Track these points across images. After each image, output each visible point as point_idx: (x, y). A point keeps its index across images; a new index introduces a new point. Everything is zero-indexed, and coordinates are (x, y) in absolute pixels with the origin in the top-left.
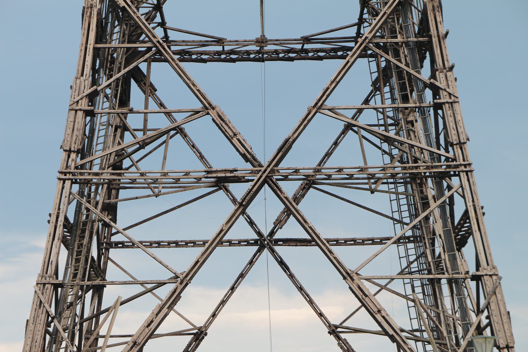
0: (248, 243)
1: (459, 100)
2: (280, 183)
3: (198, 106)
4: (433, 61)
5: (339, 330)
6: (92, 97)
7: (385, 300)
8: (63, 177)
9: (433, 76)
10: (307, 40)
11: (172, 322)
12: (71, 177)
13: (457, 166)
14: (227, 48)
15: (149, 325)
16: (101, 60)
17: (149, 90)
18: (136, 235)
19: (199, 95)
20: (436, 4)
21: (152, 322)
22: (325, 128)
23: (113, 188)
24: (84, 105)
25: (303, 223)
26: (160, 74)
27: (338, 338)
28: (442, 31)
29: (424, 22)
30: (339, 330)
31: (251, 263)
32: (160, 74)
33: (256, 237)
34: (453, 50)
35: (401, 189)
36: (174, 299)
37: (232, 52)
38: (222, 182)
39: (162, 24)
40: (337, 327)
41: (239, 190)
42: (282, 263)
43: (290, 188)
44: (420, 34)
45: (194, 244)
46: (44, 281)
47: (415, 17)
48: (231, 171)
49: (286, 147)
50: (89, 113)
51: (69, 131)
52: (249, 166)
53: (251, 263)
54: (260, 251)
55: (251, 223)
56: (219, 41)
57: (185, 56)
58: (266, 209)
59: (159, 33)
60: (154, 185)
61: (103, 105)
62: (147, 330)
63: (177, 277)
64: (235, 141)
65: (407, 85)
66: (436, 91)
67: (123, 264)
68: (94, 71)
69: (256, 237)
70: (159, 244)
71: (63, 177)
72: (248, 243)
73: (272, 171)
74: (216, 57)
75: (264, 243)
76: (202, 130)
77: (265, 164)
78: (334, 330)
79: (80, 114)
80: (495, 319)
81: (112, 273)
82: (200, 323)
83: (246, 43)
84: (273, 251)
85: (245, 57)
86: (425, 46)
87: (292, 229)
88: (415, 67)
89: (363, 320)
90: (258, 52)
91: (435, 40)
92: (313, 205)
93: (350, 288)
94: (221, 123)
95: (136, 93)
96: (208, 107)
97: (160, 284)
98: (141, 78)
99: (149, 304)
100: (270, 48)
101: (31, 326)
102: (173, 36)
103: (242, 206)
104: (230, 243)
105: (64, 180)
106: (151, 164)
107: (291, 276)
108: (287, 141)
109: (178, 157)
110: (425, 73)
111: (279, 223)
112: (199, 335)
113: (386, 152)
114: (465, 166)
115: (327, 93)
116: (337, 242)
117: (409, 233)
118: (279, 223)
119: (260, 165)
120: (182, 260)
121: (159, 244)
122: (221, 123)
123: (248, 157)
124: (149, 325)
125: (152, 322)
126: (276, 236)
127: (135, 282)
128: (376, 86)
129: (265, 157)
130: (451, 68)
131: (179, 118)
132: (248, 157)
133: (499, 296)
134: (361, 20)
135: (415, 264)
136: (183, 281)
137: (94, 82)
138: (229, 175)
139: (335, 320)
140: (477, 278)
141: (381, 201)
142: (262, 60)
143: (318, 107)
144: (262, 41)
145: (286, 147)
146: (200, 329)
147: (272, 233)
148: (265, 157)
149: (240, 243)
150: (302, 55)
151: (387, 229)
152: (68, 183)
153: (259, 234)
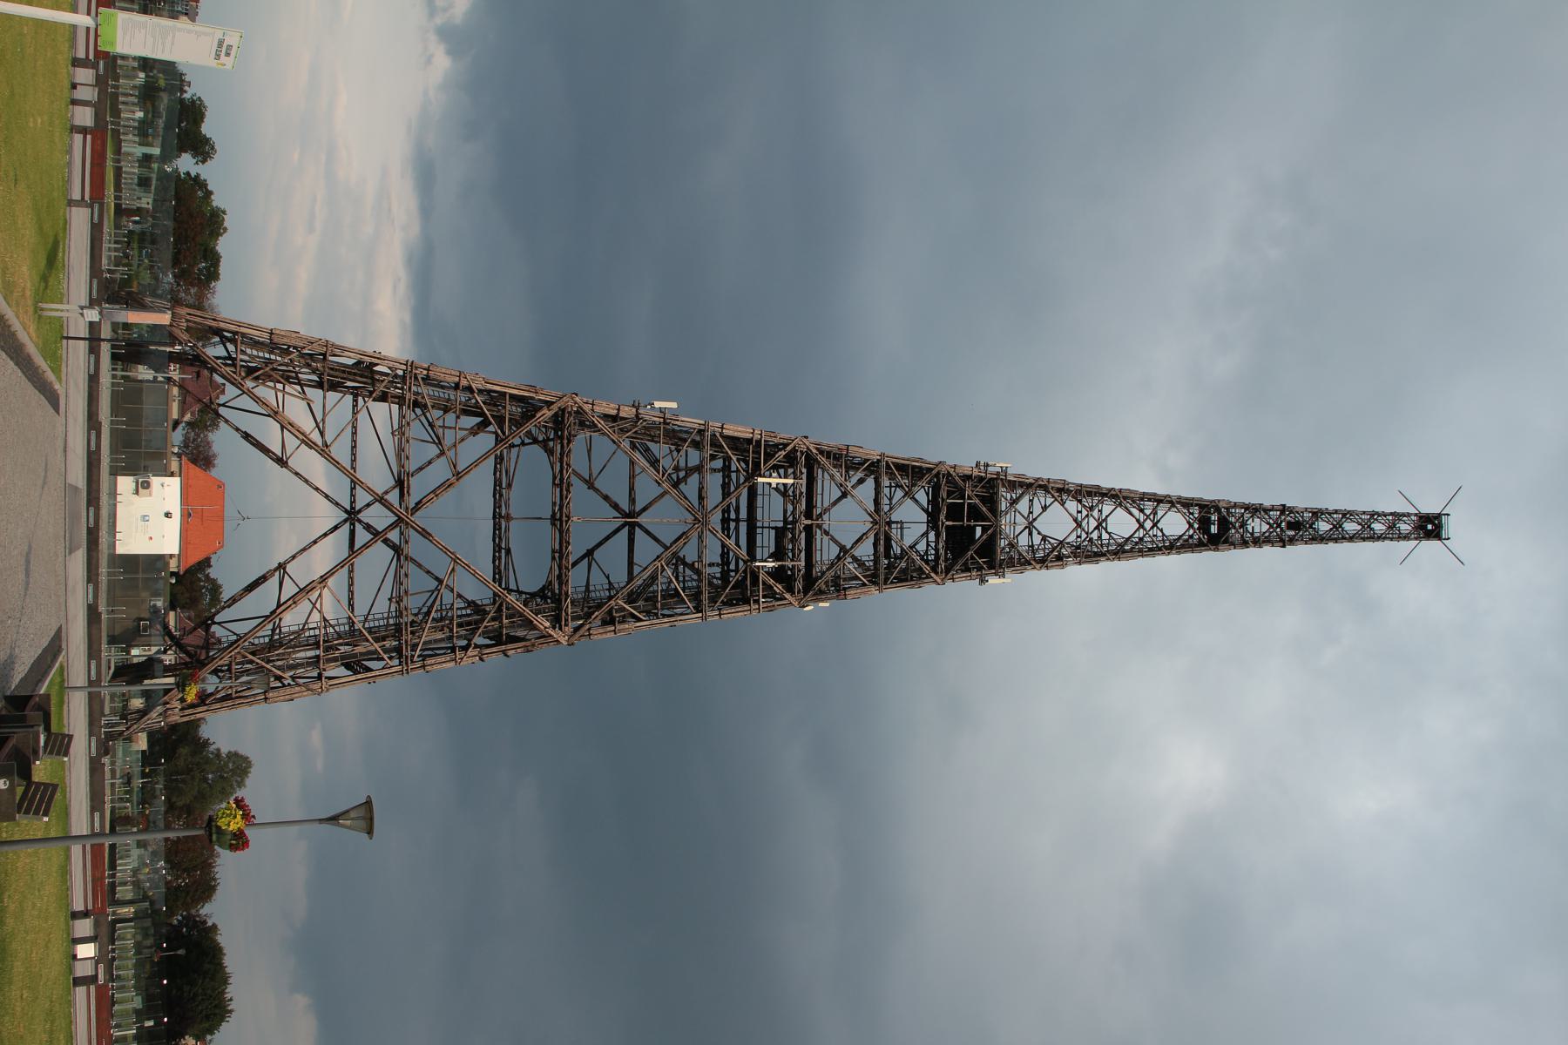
0: (353, 502)
3: (460, 468)
4: (488, 646)
6: (469, 389)
7: (305, 606)
9: (476, 646)
10: (508, 551)
11: (292, 443)
16: (495, 398)
17: (474, 431)
18: (363, 416)
19: (468, 470)
23: (401, 400)
24: (464, 383)
25: (366, 546)
26: (486, 441)
31: (337, 504)
32: (486, 441)
34: (494, 658)
35: (391, 621)
36: (311, 444)
38: (401, 484)
39: (523, 444)
41: (393, 498)
42: (336, 528)
43: (394, 536)
47: (520, 633)
49: (425, 534)
50: (457, 386)
52: (412, 505)
53: (337, 504)
54: (346, 511)
55: (368, 505)
56: (509, 486)
57: (499, 459)
58: (378, 517)
59: (517, 441)
60: (400, 431)
61: (463, 396)
65: (472, 627)
66: (465, 649)
67: (339, 405)
68: (489, 391)
70: (354, 433)
72: (353, 502)
74: (498, 482)
75: (352, 515)
76: (440, 472)
80: (288, 690)
81: (333, 396)
83: (507, 506)
84: (345, 521)
85: (497, 505)
86: (499, 639)
87: (362, 536)
89: (289, 590)
92: (380, 555)
94: (447, 485)
95: (470, 421)
96: (458, 475)
97: (322, 434)
98: (485, 424)
99: (307, 425)
102: (514, 451)
103: (381, 499)
104: (353, 489)
106: (417, 430)
109: (422, 451)
110: (478, 640)
111: (368, 527)
112: (282, 462)
115: (467, 567)
116: (351, 571)
118: (368, 527)
120: (341, 452)
121: (354, 433)
122: (447, 485)
123: (419, 505)
127: (324, 415)
128: (471, 604)
129: (419, 519)
131: (451, 454)
132: (419, 505)
134: (520, 593)
136: (324, 451)
137: (480, 391)
139: (289, 568)
140: (320, 677)
141: (382, 606)
143: (455, 560)
144: (508, 518)
145: (425, 534)
147: (360, 521)
149: (353, 495)
150: (497, 548)
151: (361, 609)
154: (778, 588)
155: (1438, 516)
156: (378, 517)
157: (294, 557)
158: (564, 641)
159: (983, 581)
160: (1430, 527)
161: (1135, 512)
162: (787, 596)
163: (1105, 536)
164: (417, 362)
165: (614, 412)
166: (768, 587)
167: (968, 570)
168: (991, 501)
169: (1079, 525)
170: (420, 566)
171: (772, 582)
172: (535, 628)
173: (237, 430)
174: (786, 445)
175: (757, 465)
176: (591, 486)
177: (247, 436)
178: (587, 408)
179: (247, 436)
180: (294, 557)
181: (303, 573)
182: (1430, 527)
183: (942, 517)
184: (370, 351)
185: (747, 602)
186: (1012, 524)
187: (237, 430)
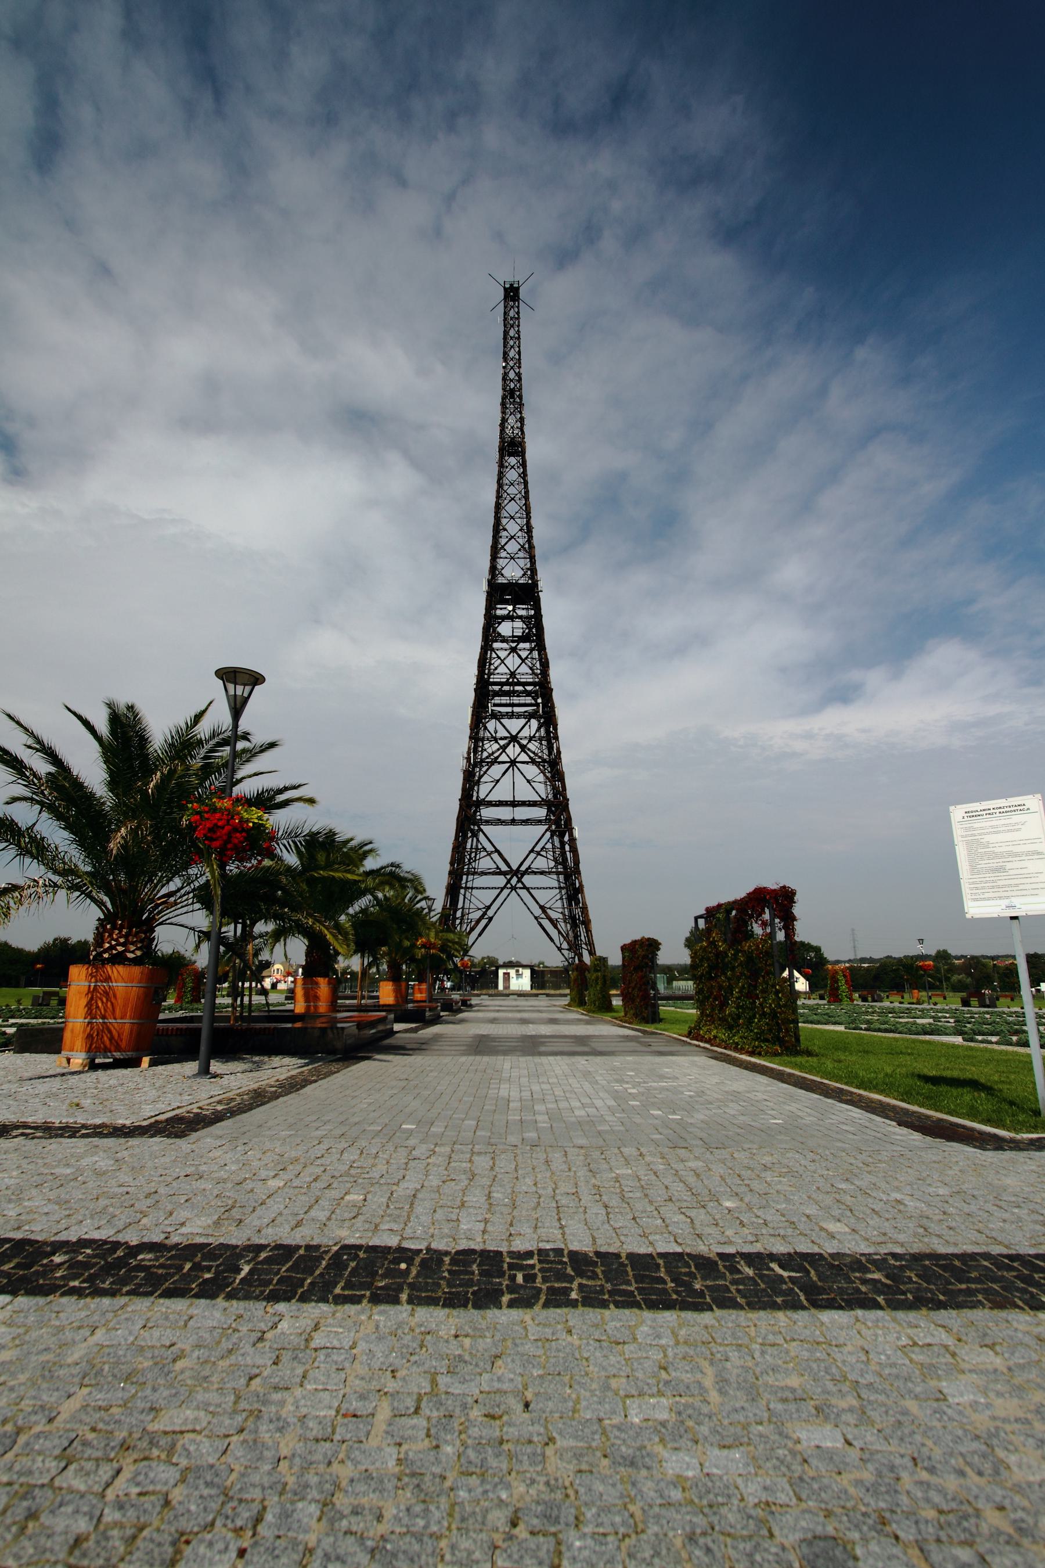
22: (533, 855)
75: (514, 888)
76: (495, 856)
94: (500, 854)
96: (497, 851)
103: (509, 881)
112: (490, 919)
122: (500, 854)
129: (514, 868)
136: (488, 908)
143: (532, 851)
148: (514, 868)
155: (505, 288)
156: (514, 880)
160: (512, 294)
161: (506, 502)
163: (518, 515)
169: (512, 537)
176: (498, 781)
177: (480, 935)
179: (480, 935)
181: (538, 912)
182: (512, 294)
186: (513, 572)
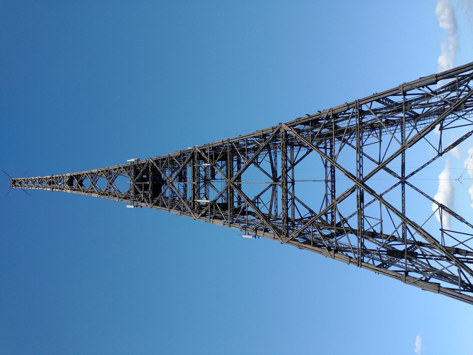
1: (331, 108)
2: (364, 177)
5: (440, 152)
8: (360, 265)
12: (360, 262)
13: (357, 106)
14: (329, 192)
15: (426, 237)
20: (298, 120)
21: (424, 235)
24: (332, 253)
27: (444, 152)
28: (307, 117)
29: (305, 124)
30: (440, 152)
31: (411, 186)
33: (401, 184)
34: (313, 112)
37: (331, 191)
40: (439, 153)
44: (308, 125)
45: (403, 208)
46: (404, 280)
48: (358, 197)
51: (342, 260)
53: (411, 186)
56: (326, 196)
62: (428, 238)
63: (404, 223)
64: (346, 195)
69: (401, 184)
71: (360, 265)
73: (358, 180)
77: (355, 184)
78: (440, 154)
79: (336, 255)
80: (423, 83)
82: (437, 206)
84: (407, 178)
88: (320, 125)
90: (332, 182)
91: (310, 119)
93: (409, 147)
100: (329, 178)
101: (425, 288)
105: (361, 265)
107: (417, 171)
108: (346, 175)
113: (368, 137)
114: (356, 103)
117: (399, 127)
119: (356, 185)
123: (353, 190)
124: (426, 237)
125: (424, 235)
126: (401, 176)
129: (352, 184)
130: (320, 112)
132: (353, 190)
133: (412, 83)
135: (412, 124)
138: (359, 198)
140: (405, 94)
142: (335, 181)
146: (439, 207)
147: (399, 178)
148: (352, 184)
152: (363, 264)
153: (400, 183)
154: (203, 155)
157: (434, 159)
158: (283, 125)
159: (138, 160)
162: (200, 151)
164: (355, 267)
165: (266, 233)
166: (206, 154)
167: (143, 164)
168: (136, 192)
170: (368, 157)
171: (205, 157)
172: (296, 130)
173: (467, 223)
174: (201, 216)
175: (212, 207)
177: (462, 220)
178: (277, 236)
179: (462, 220)
180: (434, 159)
183: (150, 186)
184: (381, 275)
185: (214, 148)
187: (467, 223)
